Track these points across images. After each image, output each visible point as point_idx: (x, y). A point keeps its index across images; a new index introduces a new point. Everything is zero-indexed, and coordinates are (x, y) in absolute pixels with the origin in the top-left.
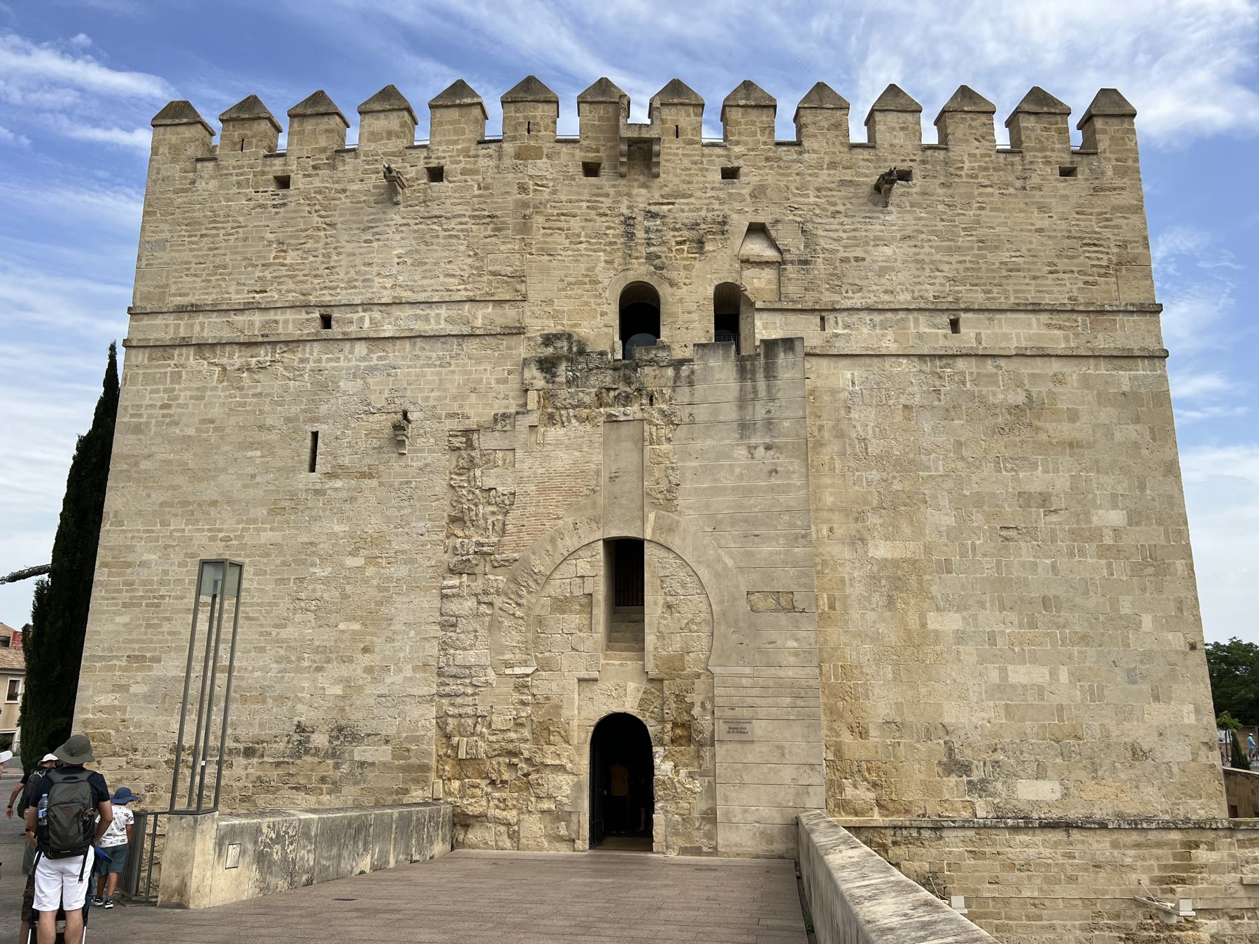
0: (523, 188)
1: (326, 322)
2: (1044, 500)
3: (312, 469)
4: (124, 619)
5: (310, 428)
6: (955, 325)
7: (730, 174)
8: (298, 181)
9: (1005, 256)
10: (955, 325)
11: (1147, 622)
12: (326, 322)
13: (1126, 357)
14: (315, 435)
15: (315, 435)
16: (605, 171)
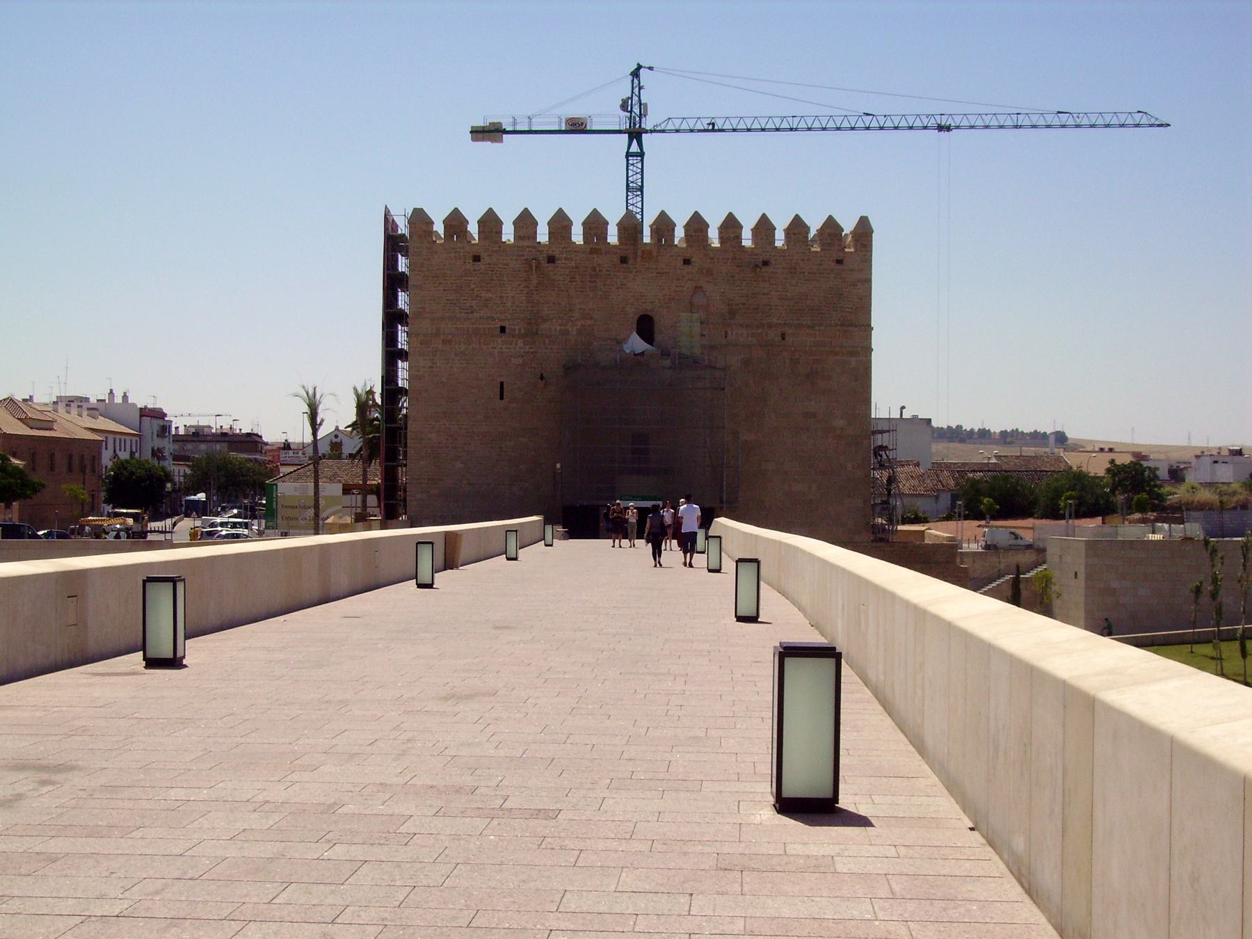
0: (594, 269)
1: (503, 329)
2: (814, 415)
3: (502, 398)
4: (422, 463)
5: (499, 380)
6: (783, 336)
7: (687, 262)
8: (486, 259)
9: (809, 302)
10: (783, 336)
11: (849, 466)
12: (503, 329)
13: (852, 354)
14: (502, 384)
15: (502, 384)
16: (630, 262)
